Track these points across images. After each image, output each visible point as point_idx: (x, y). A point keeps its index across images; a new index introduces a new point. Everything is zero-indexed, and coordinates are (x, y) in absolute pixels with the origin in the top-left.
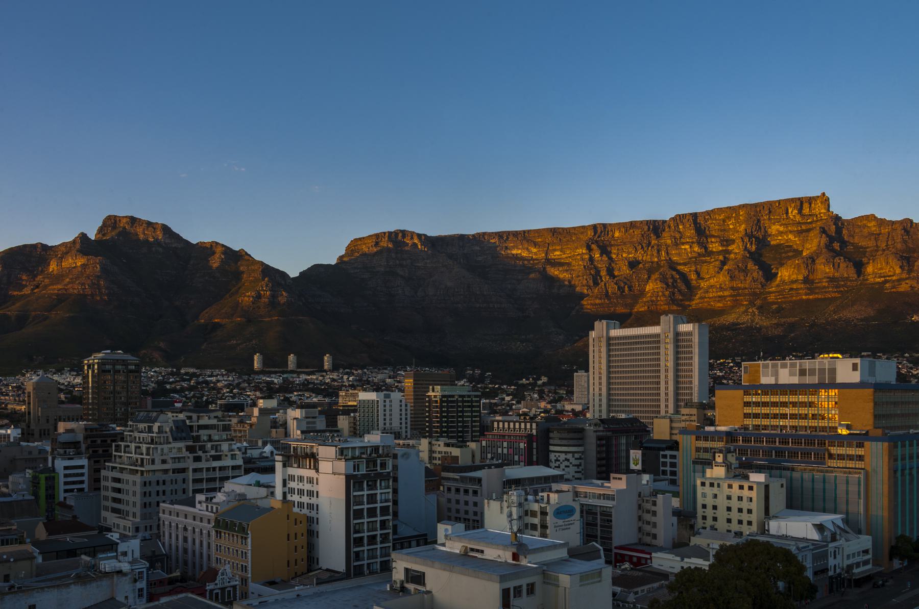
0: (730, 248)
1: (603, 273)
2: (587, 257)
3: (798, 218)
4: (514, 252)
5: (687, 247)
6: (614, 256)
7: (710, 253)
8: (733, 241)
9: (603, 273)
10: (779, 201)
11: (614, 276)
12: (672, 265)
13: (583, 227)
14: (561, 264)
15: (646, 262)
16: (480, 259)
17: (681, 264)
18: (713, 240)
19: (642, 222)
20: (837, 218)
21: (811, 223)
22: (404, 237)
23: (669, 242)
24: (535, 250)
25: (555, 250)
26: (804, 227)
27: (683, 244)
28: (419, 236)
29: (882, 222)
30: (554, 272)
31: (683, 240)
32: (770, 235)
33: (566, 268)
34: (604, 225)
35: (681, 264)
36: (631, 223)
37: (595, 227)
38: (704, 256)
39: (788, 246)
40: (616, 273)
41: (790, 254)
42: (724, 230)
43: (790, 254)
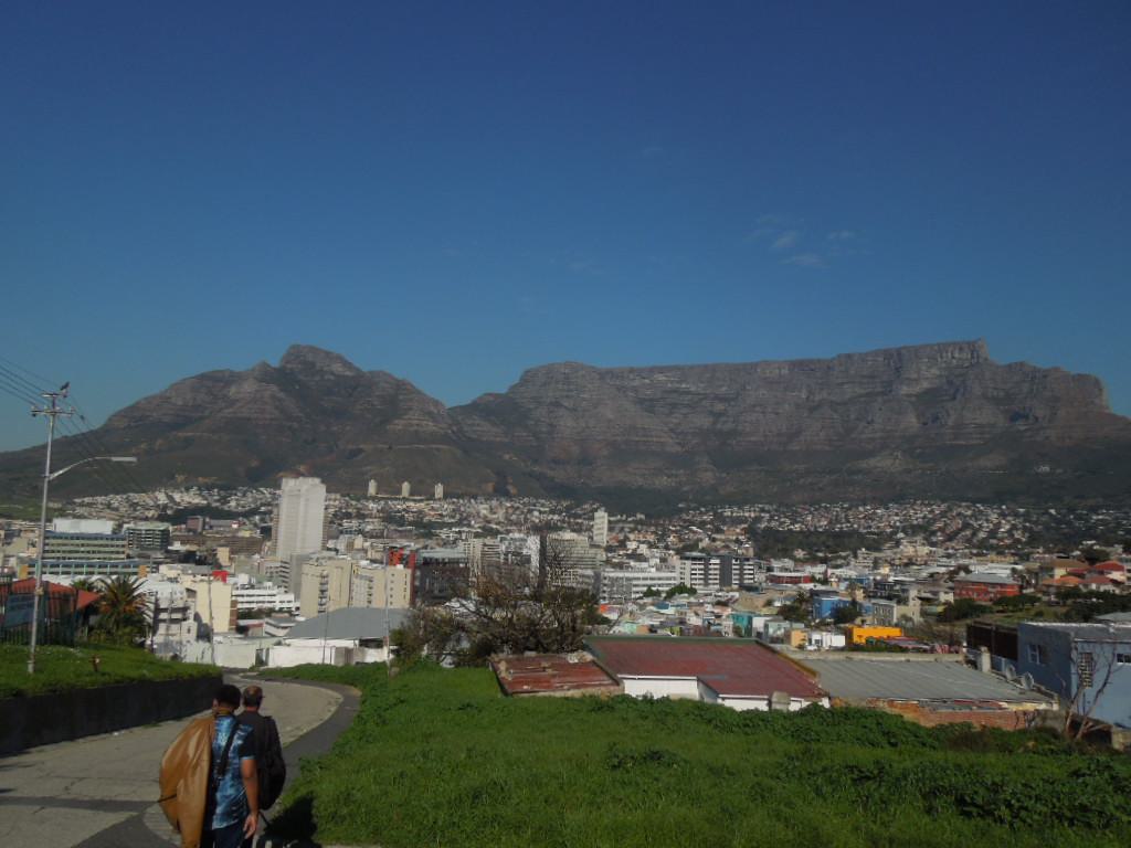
5: (846, 386)
11: (777, 414)
25: (721, 386)
27: (843, 384)
30: (720, 407)
35: (838, 404)
40: (780, 411)
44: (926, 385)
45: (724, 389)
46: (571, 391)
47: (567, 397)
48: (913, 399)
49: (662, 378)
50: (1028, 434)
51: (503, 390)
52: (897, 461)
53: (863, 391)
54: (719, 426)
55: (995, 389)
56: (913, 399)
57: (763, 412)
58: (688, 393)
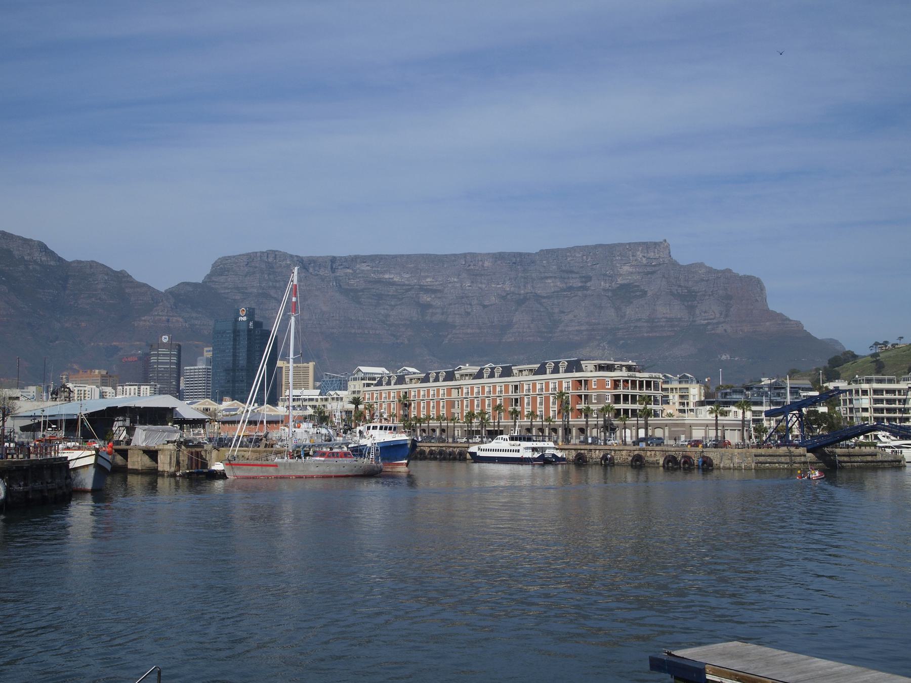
0: (588, 284)
1: (475, 302)
2: (458, 285)
3: (644, 261)
4: (387, 276)
5: (549, 281)
6: (484, 286)
7: (570, 289)
8: (589, 279)
9: (475, 302)
10: (629, 244)
11: (485, 307)
12: (538, 298)
13: (455, 255)
14: (434, 291)
15: (513, 293)
16: (352, 282)
17: (544, 297)
18: (574, 276)
19: (509, 254)
20: (675, 264)
21: (654, 266)
22: (275, 258)
23: (534, 275)
24: (407, 276)
25: (428, 277)
26: (649, 269)
27: (547, 278)
28: (291, 256)
29: (710, 271)
30: (426, 298)
31: (546, 275)
32: (621, 275)
33: (439, 295)
34: (473, 255)
35: (544, 297)
36: (500, 254)
37: (465, 255)
38: (564, 290)
39: (638, 286)
40: (486, 303)
41: (638, 293)
42: (582, 267)
43: (638, 293)
44: (620, 281)
45: (429, 280)
46: (276, 281)
47: (275, 287)
48: (610, 294)
49: (364, 267)
50: (709, 327)
51: (199, 279)
52: (607, 352)
53: (563, 286)
54: (428, 318)
55: (680, 286)
56: (610, 294)
57: (471, 304)
58: (393, 284)
